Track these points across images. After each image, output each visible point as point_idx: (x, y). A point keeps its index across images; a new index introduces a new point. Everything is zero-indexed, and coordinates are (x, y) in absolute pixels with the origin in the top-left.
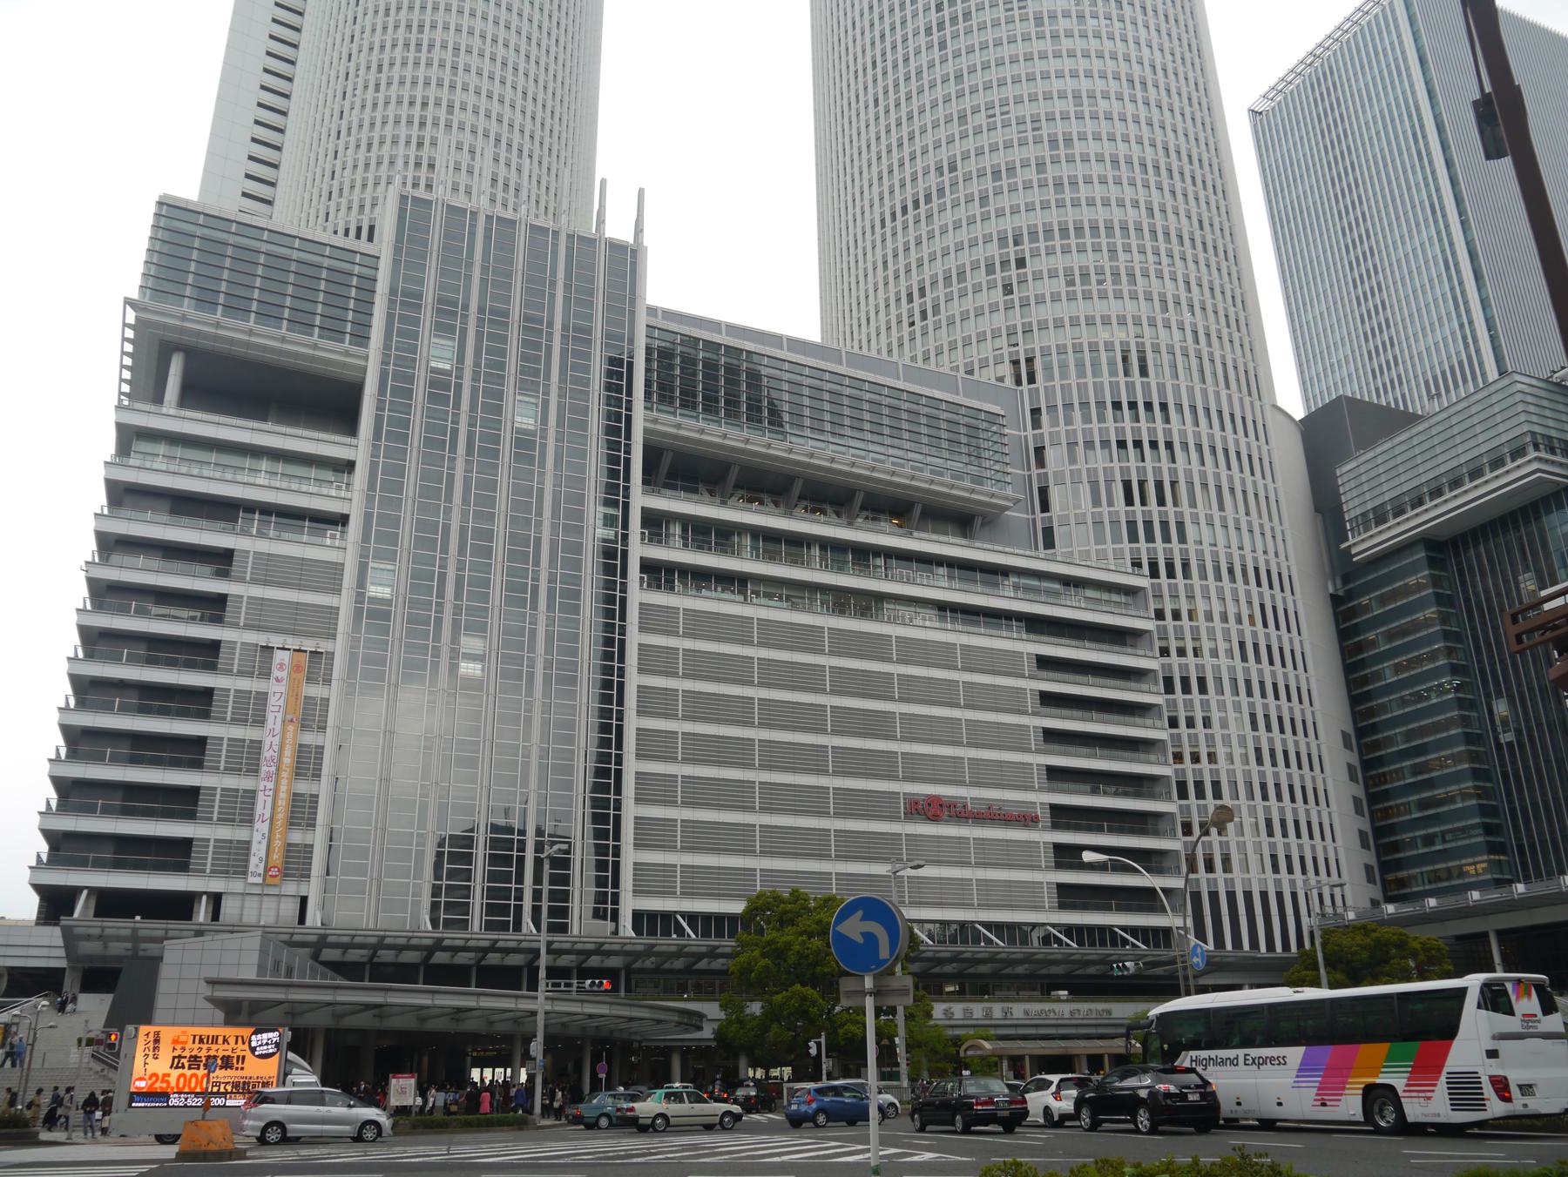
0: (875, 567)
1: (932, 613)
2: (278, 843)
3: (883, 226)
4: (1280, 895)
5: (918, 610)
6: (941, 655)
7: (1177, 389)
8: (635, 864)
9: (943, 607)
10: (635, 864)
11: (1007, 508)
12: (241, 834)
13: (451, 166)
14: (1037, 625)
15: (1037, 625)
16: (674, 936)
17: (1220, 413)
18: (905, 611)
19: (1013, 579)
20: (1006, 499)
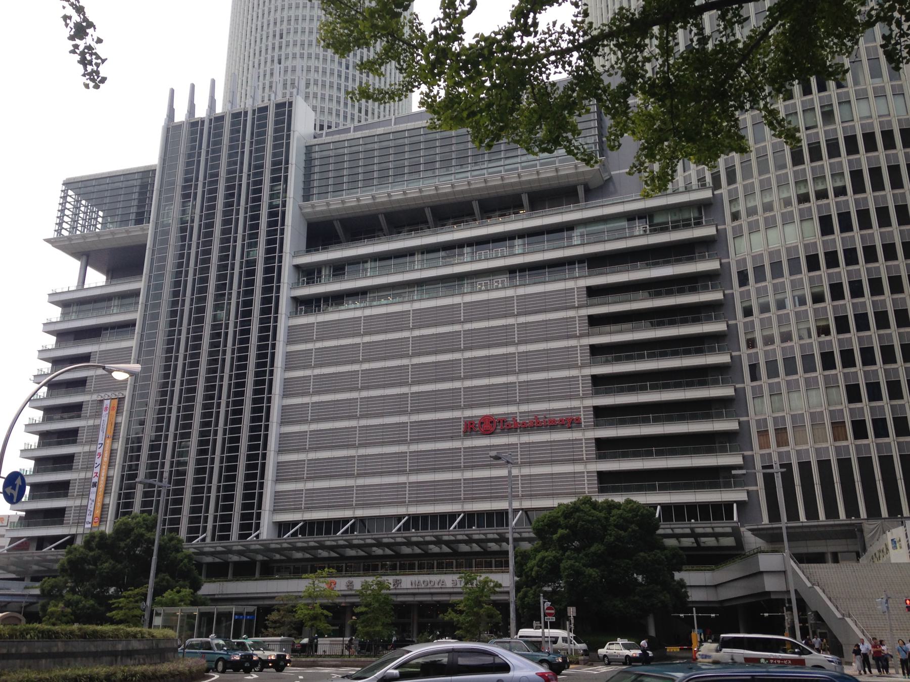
1: (504, 279)
2: (99, 505)
5: (491, 278)
9: (512, 271)
12: (84, 502)
13: (305, 69)
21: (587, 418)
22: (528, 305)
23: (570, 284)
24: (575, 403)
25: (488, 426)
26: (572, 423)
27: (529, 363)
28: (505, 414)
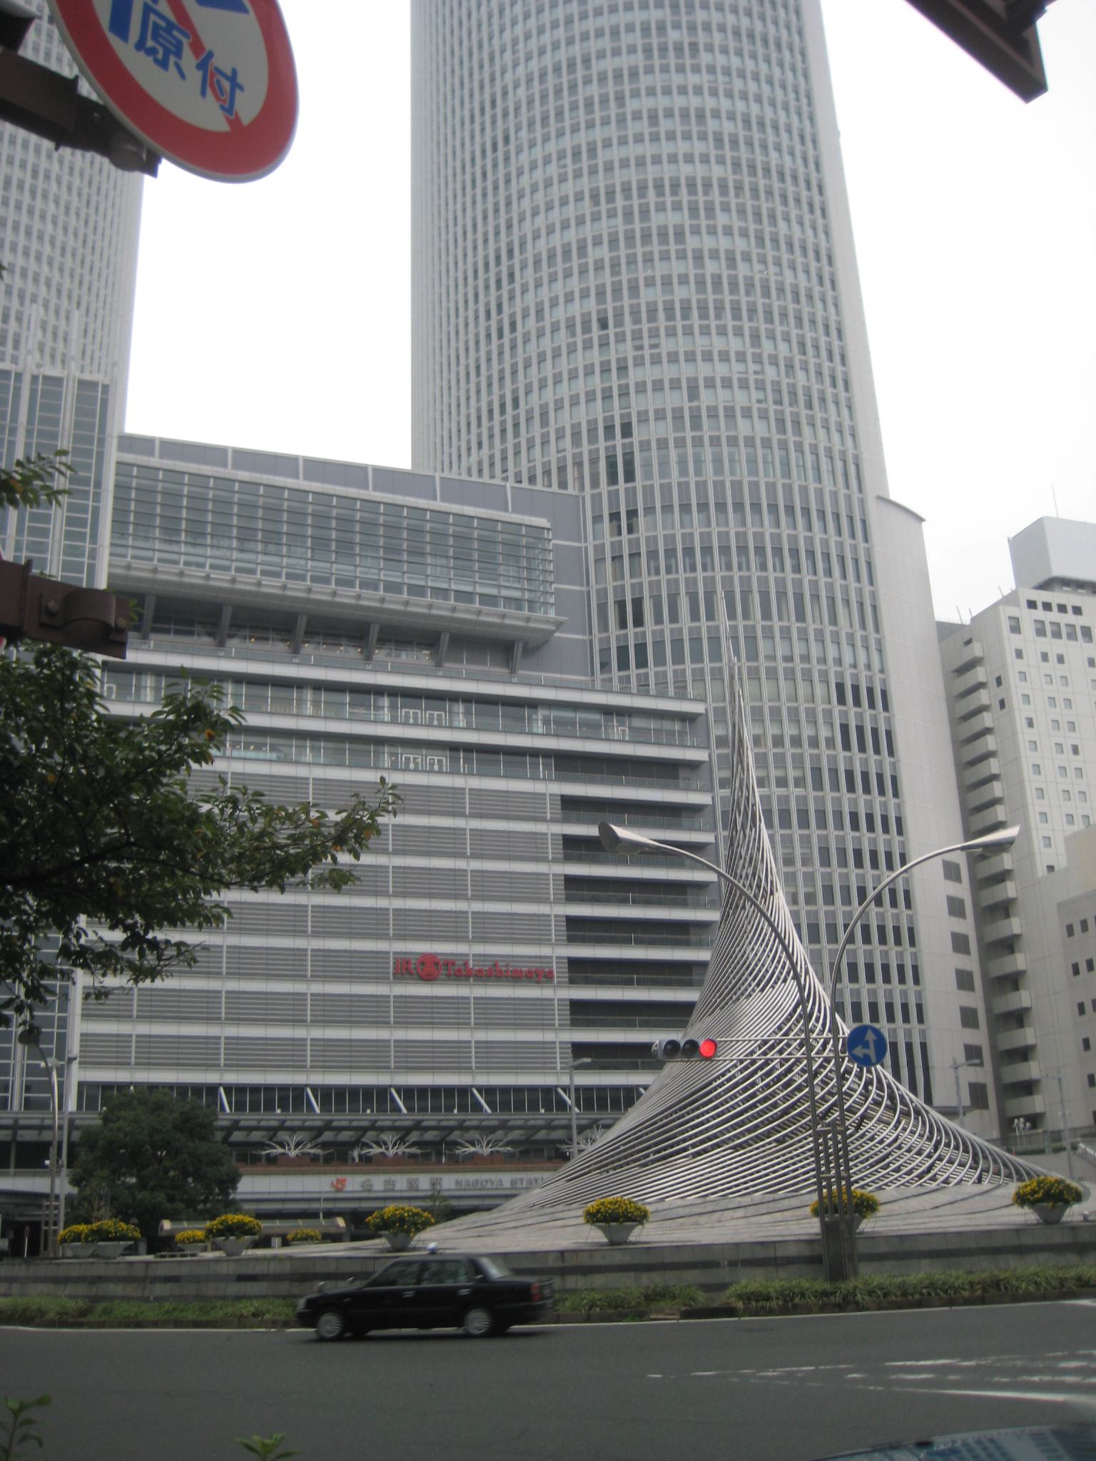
0: (378, 708)
3: (500, 336)
4: (909, 1047)
6: (449, 802)
7: (820, 493)
8: (82, 1035)
10: (82, 1035)
11: (554, 632)
14: (568, 764)
15: (568, 764)
16: (279, 1111)
17: (851, 519)
18: (404, 755)
19: (541, 713)
20: (548, 622)
21: (560, 971)
22: (485, 805)
23: (539, 787)
24: (545, 951)
25: (428, 969)
26: (539, 975)
27: (486, 886)
28: (452, 954)
